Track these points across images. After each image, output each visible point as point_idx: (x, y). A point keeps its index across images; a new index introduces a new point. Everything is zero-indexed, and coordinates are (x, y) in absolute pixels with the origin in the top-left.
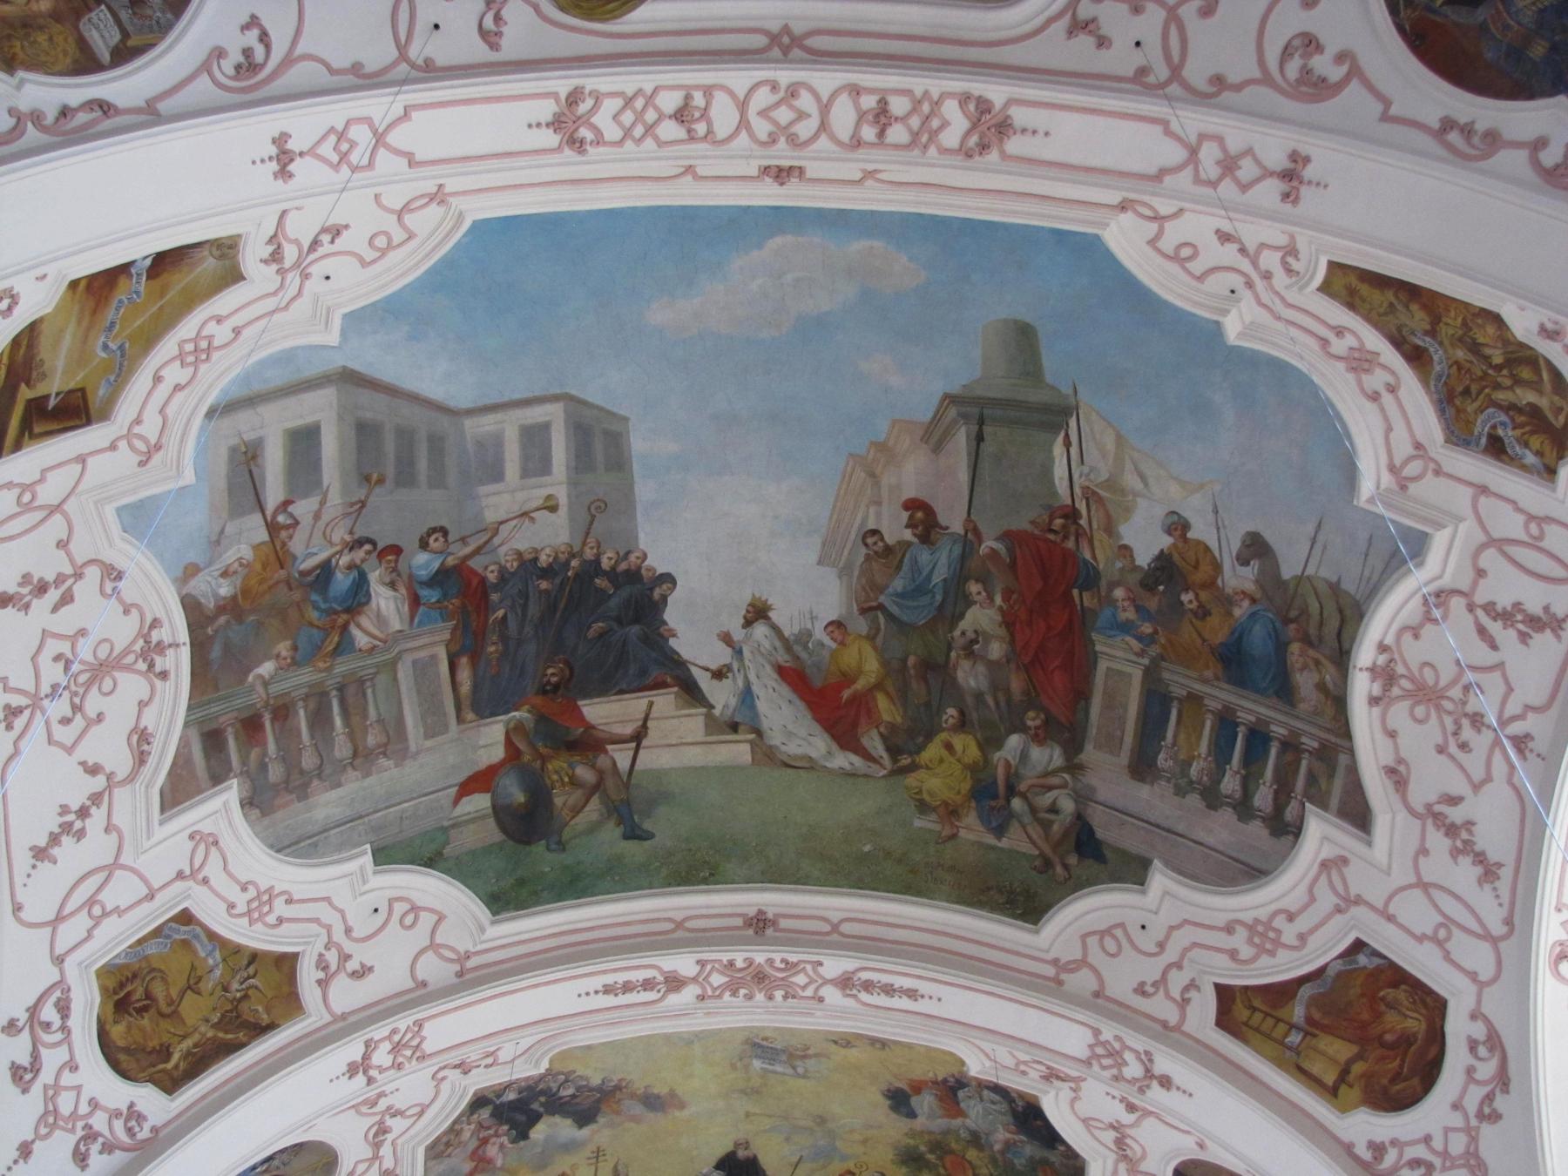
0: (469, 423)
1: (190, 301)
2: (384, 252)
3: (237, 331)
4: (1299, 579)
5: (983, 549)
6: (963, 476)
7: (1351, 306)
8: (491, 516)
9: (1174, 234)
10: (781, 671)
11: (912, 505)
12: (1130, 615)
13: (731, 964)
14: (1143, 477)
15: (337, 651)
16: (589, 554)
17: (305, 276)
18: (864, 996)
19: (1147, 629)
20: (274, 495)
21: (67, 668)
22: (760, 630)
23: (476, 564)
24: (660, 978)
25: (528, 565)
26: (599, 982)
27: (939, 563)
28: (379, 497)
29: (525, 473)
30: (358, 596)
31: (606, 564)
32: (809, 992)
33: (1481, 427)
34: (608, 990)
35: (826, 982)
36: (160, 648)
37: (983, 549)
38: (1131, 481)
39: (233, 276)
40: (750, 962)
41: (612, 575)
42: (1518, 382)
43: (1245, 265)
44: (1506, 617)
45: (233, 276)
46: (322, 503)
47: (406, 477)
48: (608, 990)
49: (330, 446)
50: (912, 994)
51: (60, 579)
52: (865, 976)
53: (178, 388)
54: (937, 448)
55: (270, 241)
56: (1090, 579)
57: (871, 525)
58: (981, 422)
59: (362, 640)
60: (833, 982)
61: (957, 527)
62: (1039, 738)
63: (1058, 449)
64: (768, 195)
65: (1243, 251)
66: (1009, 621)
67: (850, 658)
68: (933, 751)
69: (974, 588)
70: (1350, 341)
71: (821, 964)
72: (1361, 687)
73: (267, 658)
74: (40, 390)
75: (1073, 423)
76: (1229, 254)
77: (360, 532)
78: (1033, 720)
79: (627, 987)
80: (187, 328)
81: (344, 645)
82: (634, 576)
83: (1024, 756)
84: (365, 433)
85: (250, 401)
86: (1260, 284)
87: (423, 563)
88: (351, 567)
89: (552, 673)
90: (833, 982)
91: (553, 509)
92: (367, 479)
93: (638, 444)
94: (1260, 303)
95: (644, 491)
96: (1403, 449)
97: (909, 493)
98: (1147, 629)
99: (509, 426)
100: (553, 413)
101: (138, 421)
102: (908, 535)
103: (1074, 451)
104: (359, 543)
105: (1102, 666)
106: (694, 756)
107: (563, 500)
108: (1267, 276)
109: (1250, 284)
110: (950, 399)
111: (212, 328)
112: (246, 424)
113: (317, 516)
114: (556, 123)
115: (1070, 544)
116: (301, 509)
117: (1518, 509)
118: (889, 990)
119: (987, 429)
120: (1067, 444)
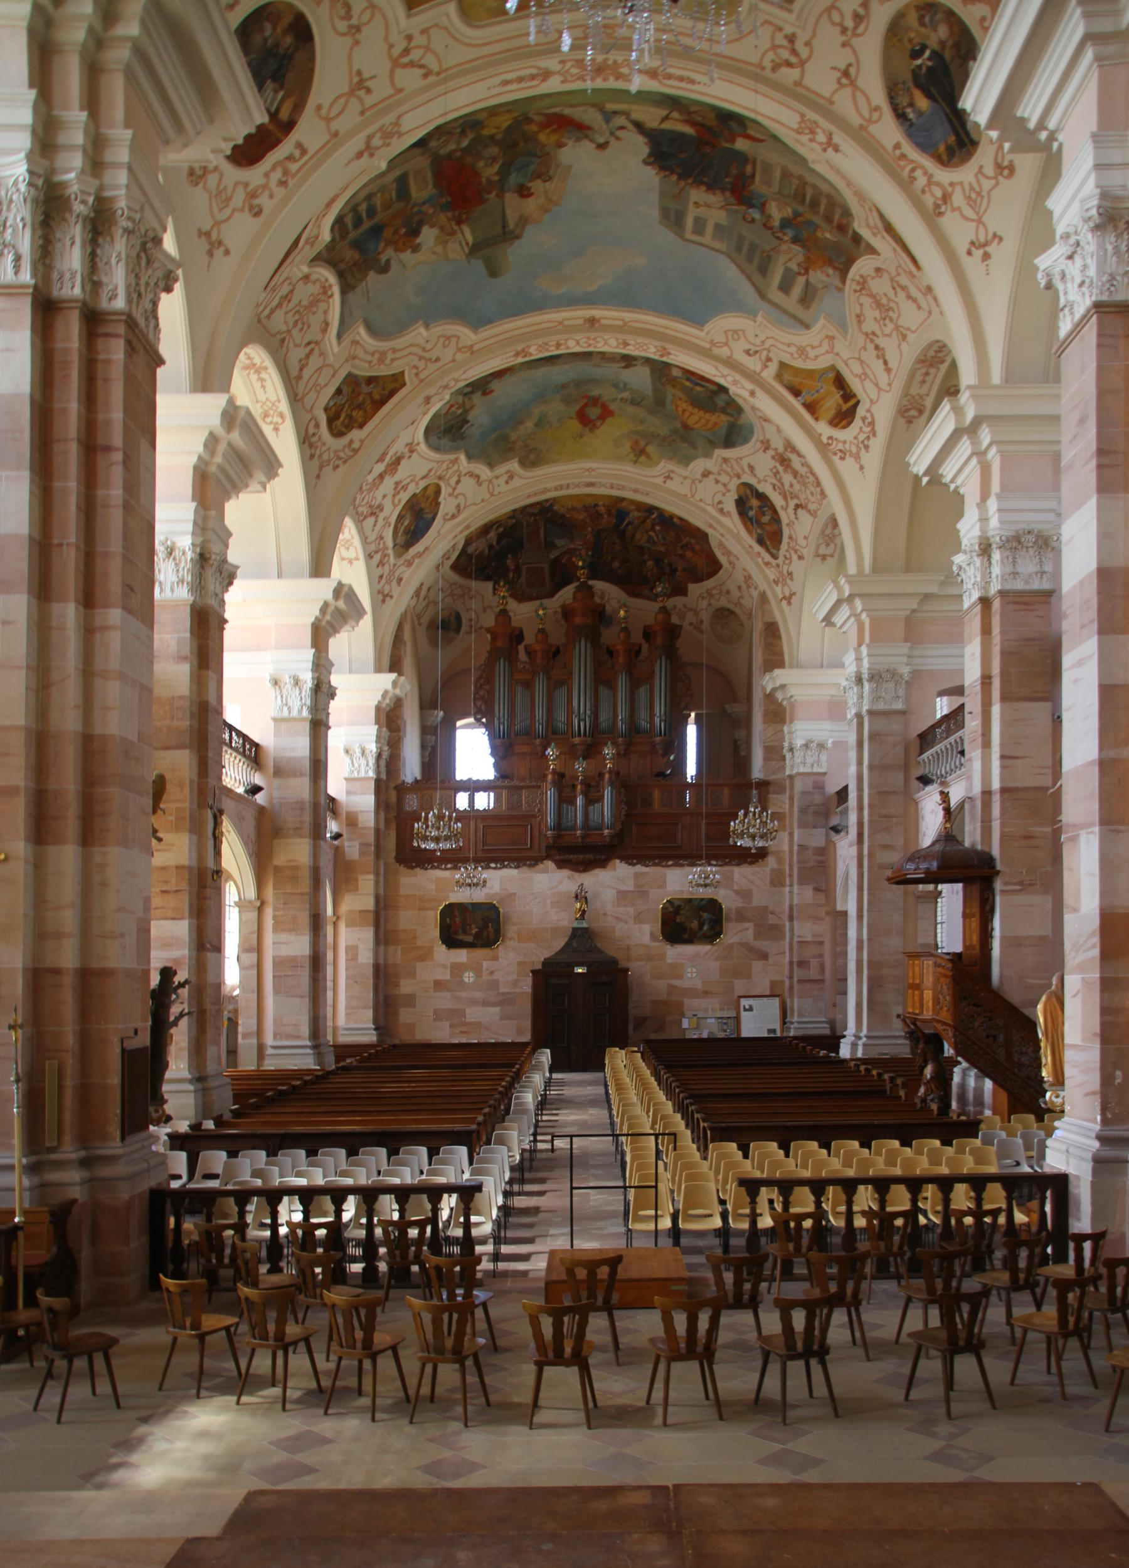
0: (723, 247)
1: (797, 371)
2: (735, 332)
3: (789, 345)
4: (366, 276)
5: (494, 194)
6: (508, 212)
7: (394, 375)
8: (723, 213)
9: (451, 349)
10: (589, 128)
11: (530, 195)
12: (424, 209)
13: (617, 79)
14: (434, 253)
15: (800, 215)
16: (682, 183)
17: (763, 342)
18: (534, 71)
19: (416, 210)
20: (801, 281)
21: (884, 319)
22: (601, 140)
23: (732, 200)
24: (660, 77)
25: (711, 188)
26: (696, 87)
27: (513, 179)
28: (767, 247)
29: (705, 221)
30: (786, 223)
31: (674, 178)
32: (568, 65)
33: (345, 389)
34: (693, 82)
35: (558, 73)
36: (858, 283)
37: (494, 194)
38: (439, 249)
39: (783, 365)
40: (605, 80)
41: (673, 172)
42: (347, 416)
43: (427, 355)
44: (308, 356)
45: (783, 365)
46: (786, 262)
47: (753, 248)
48: (693, 82)
49: (777, 279)
50: (506, 83)
51: (872, 341)
52: (535, 83)
53: (813, 348)
54: (521, 217)
55: (766, 367)
56: (445, 208)
57: (548, 183)
58: (504, 233)
59: (790, 210)
60: (554, 73)
61: (509, 197)
62: (454, 151)
63: (470, 239)
64: (597, 313)
65: (430, 360)
66: (477, 175)
67: (554, 138)
68: (506, 125)
69: (496, 178)
70: (388, 362)
71: (563, 82)
72: (333, 280)
73: (826, 239)
74: (841, 402)
75: (467, 251)
76: (433, 355)
77: (777, 242)
78: (458, 154)
79: (681, 79)
80: (799, 364)
81: (797, 214)
82: (663, 168)
83: (458, 143)
84: (764, 270)
85: (795, 318)
86: (421, 353)
87: (755, 214)
88: (785, 234)
89: (707, 149)
90: (554, 73)
91: (696, 203)
92: (769, 257)
93: (655, 213)
94: (418, 345)
95: (654, 197)
96: (360, 353)
97: (531, 200)
98: (416, 210)
99: (707, 239)
100: (688, 234)
101: (827, 352)
102: (530, 185)
103: (464, 243)
104: (778, 238)
105: (431, 186)
106: (634, 107)
107: (691, 207)
108: (421, 358)
109: (424, 349)
110: (519, 237)
111: (796, 356)
112: (799, 311)
113: (790, 259)
114: (669, 354)
115: (457, 213)
116: (794, 267)
117: (326, 385)
118: (520, 80)
119: (500, 231)
120: (467, 244)
